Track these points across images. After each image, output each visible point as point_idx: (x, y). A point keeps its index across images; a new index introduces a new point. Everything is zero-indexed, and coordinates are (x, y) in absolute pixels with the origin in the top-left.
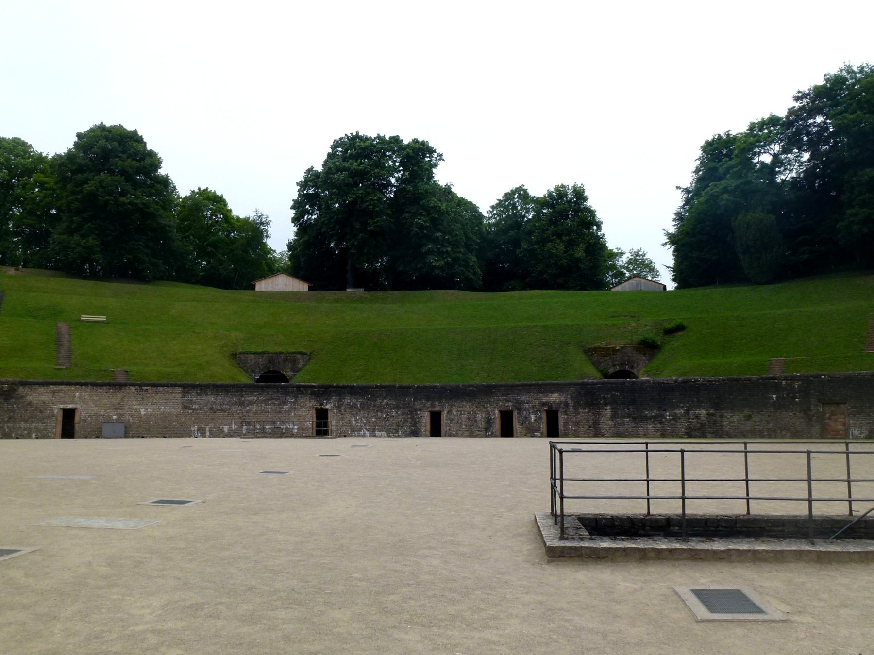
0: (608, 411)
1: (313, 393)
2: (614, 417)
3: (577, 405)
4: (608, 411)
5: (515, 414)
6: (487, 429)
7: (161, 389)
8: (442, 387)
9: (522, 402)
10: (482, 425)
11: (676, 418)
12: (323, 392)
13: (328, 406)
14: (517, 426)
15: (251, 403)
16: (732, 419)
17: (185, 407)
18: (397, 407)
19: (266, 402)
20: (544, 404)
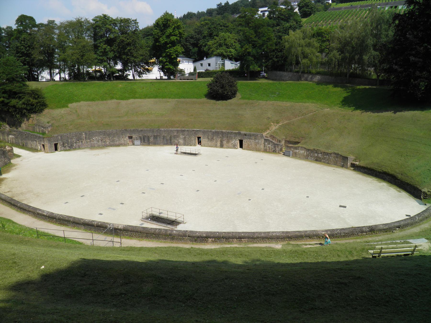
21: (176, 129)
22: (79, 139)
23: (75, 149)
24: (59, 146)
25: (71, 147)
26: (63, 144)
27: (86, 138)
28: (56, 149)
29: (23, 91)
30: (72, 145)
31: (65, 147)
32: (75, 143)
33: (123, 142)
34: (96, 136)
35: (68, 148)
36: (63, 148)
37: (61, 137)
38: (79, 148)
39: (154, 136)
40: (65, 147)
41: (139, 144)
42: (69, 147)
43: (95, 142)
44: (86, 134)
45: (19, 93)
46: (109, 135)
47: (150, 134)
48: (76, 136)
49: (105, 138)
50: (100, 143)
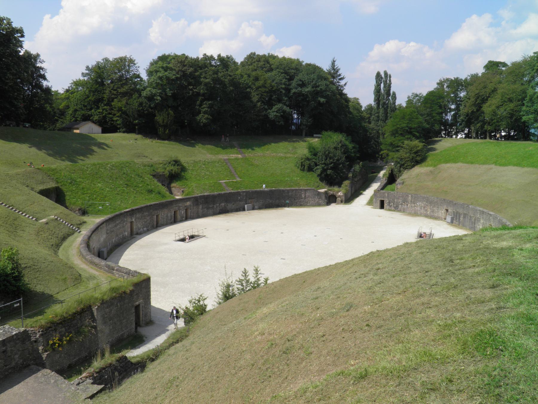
0: (201, 207)
1: (130, 215)
2: (202, 208)
3: (193, 206)
4: (201, 207)
5: (178, 212)
6: (171, 220)
7: (103, 225)
8: (160, 203)
9: (180, 207)
10: (170, 218)
11: (217, 207)
12: (132, 212)
13: (133, 220)
14: (179, 217)
15: (118, 224)
16: (230, 206)
17: (107, 233)
18: (149, 215)
19: (120, 223)
20: (185, 206)
21: (481, 209)
22: (405, 201)
23: (400, 211)
24: (385, 205)
25: (396, 208)
26: (389, 203)
27: (411, 201)
28: (382, 206)
29: (400, 144)
30: (397, 206)
31: (391, 206)
32: (401, 204)
33: (440, 215)
34: (420, 201)
35: (393, 208)
36: (388, 207)
37: (388, 194)
38: (403, 211)
39: (464, 214)
40: (391, 206)
41: (450, 221)
42: (395, 208)
43: (419, 208)
44: (412, 197)
45: (398, 147)
46: (431, 203)
47: (461, 211)
48: (402, 197)
49: (427, 206)
50: (422, 211)
